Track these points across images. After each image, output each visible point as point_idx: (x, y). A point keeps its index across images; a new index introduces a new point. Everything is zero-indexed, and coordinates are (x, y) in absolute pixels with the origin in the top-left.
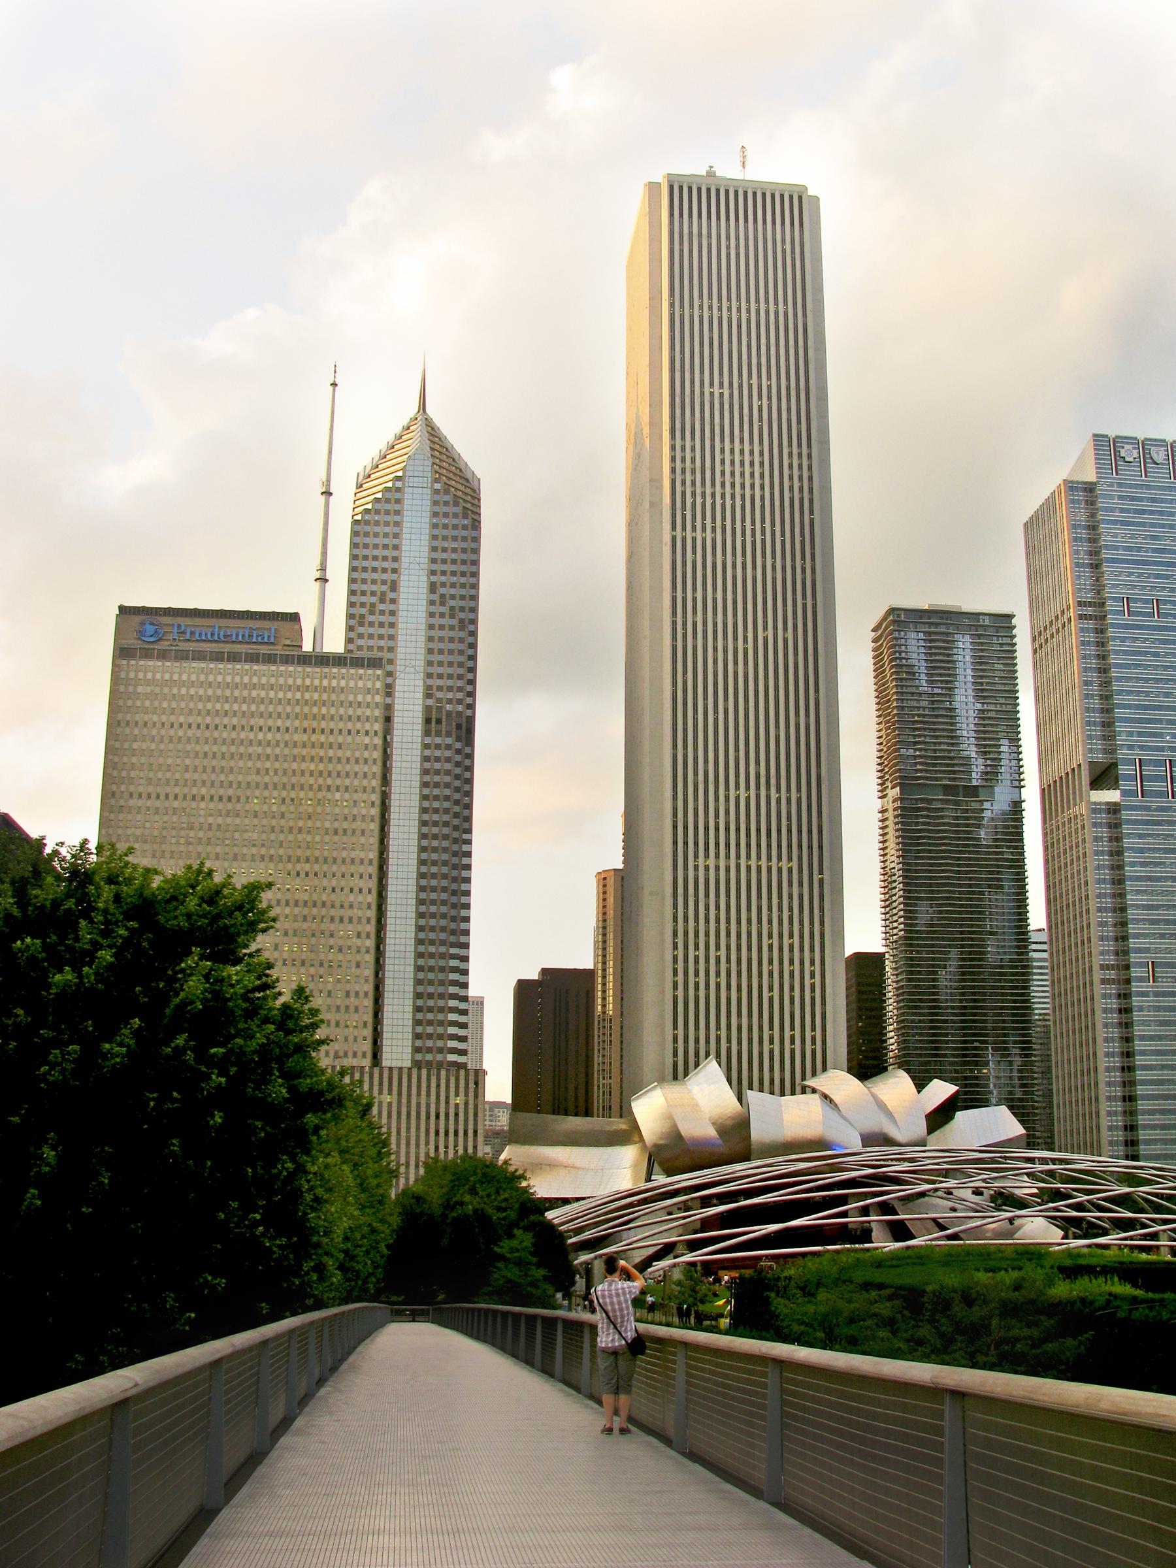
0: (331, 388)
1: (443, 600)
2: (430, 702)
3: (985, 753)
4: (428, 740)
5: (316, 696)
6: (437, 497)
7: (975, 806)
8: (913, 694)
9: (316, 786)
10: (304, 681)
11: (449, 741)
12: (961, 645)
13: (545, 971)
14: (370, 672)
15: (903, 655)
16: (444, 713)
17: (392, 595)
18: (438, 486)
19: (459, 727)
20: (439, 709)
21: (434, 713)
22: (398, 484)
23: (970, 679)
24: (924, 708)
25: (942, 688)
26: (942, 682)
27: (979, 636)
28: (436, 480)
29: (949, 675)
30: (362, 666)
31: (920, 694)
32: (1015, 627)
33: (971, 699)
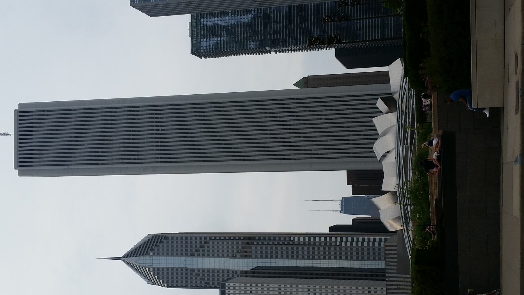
1: (197, 251)
2: (238, 256)
4: (254, 256)
6: (156, 254)
7: (272, 14)
11: (253, 248)
13: (348, 184)
14: (227, 288)
15: (211, 48)
16: (243, 250)
17: (196, 271)
18: (151, 254)
19: (248, 243)
20: (241, 252)
21: (243, 254)
22: (151, 269)
25: (223, 31)
28: (149, 255)
29: (218, 27)
33: (227, 18)
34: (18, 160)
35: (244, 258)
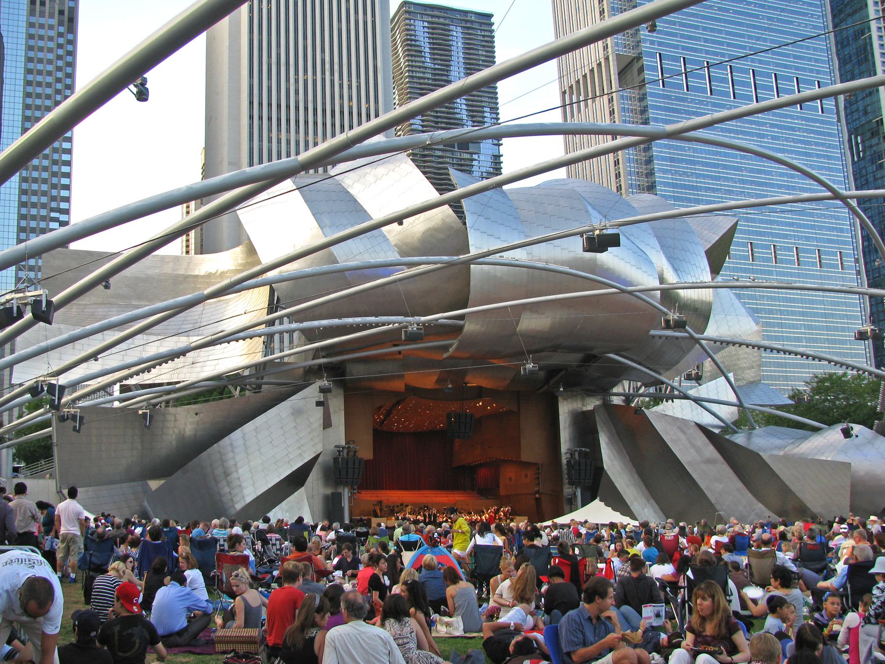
3: (473, 116)
4: (33, 19)
8: (420, 67)
12: (455, 34)
23: (461, 60)
24: (428, 79)
26: (441, 60)
27: (468, 28)
31: (426, 68)
32: (493, 24)
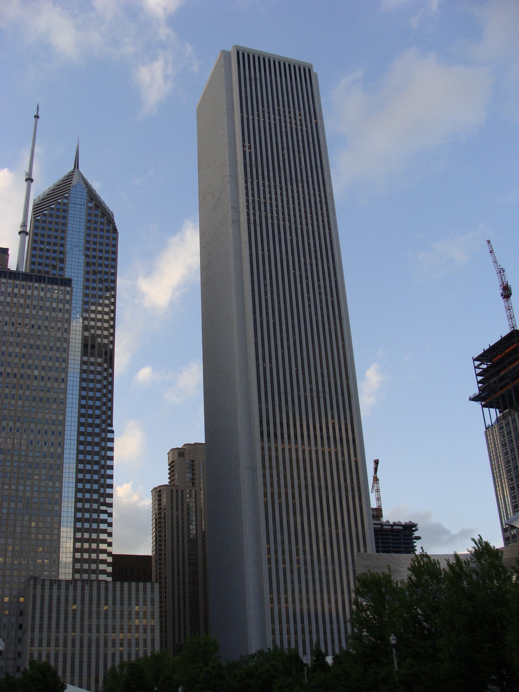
0: (34, 119)
2: (87, 334)
4: (85, 359)
5: (22, 301)
6: (90, 211)
9: (20, 365)
10: (13, 290)
11: (100, 360)
18: (91, 205)
21: (90, 341)
30: (57, 284)
34: (246, 52)
35: (83, 343)
